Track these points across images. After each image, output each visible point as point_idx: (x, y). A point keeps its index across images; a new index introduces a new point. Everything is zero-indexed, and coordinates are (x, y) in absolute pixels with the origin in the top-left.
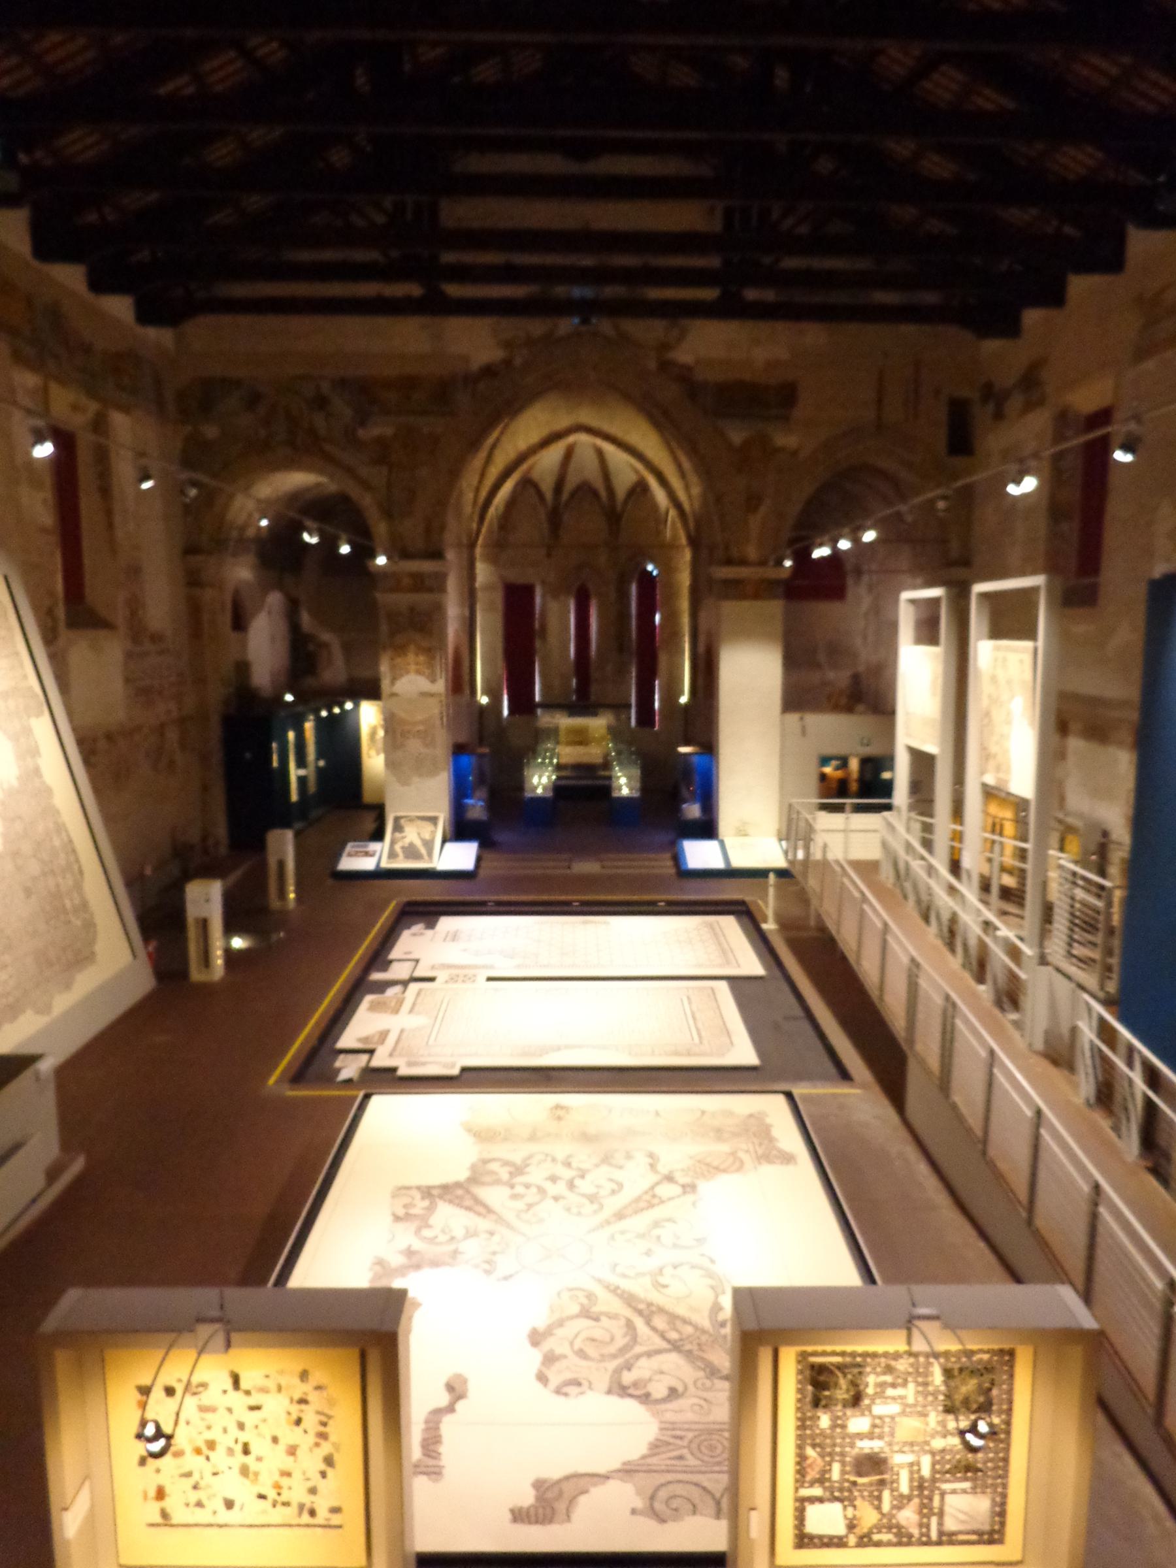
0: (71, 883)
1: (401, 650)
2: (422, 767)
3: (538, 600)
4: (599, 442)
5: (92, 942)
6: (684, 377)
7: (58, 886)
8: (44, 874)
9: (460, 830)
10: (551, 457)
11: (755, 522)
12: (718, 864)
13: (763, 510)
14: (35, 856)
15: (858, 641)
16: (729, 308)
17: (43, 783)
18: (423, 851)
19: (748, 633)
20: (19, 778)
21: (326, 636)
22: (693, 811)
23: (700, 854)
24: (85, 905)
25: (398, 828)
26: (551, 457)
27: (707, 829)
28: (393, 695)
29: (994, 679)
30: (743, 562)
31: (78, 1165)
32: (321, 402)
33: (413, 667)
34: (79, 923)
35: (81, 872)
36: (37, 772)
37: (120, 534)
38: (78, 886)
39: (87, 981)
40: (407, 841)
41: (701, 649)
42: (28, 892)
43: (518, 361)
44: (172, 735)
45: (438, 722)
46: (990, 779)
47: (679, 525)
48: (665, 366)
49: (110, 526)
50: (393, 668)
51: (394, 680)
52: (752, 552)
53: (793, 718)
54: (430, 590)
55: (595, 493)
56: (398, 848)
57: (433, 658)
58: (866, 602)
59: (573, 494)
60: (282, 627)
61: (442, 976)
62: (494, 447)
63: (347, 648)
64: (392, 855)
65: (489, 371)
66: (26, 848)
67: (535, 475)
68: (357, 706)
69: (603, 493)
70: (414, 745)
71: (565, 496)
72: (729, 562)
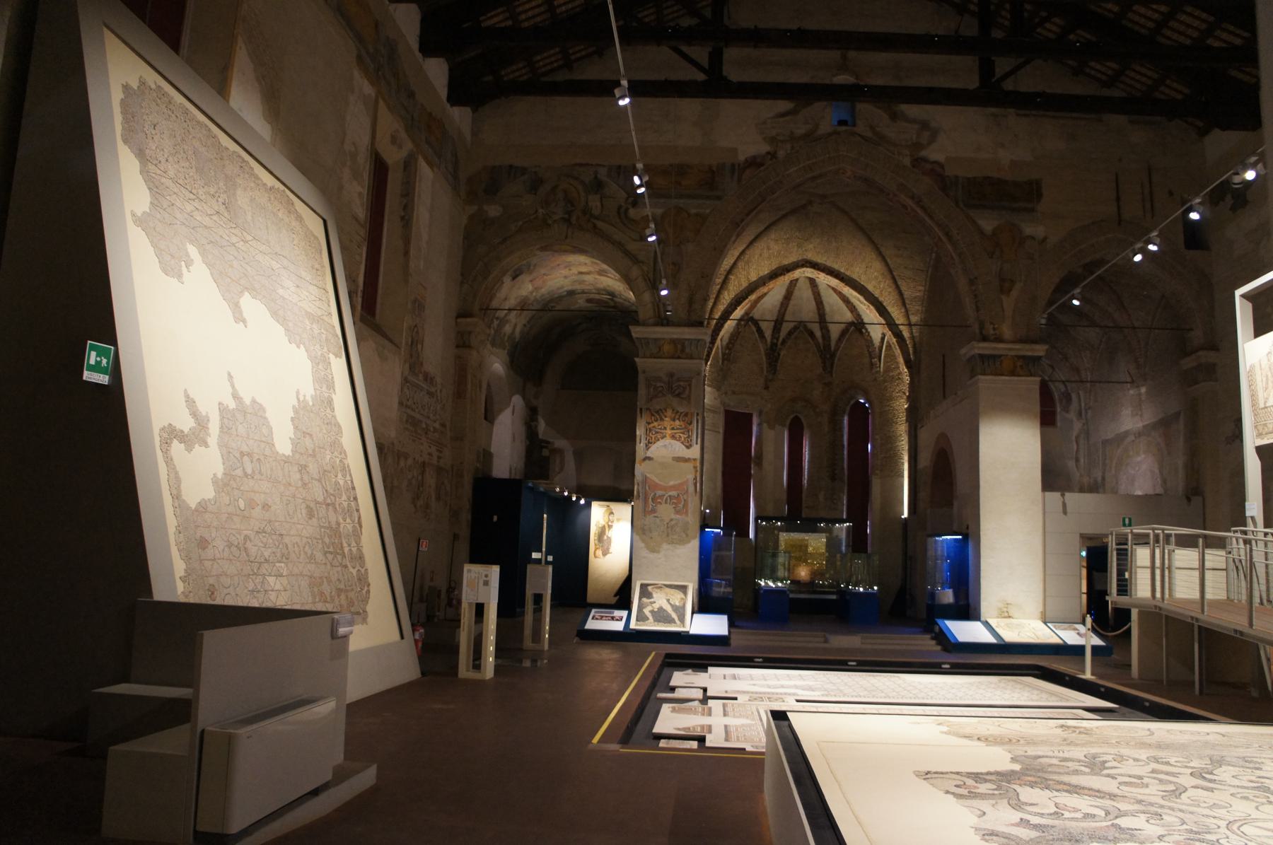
0: (350, 527)
1: (658, 414)
2: (672, 534)
3: (755, 428)
4: (823, 279)
5: (366, 600)
6: (937, 172)
9: (705, 605)
10: (776, 291)
11: (1008, 302)
12: (988, 638)
13: (1014, 293)
14: (319, 481)
15: (1071, 464)
16: (989, 94)
17: (334, 417)
18: (674, 616)
19: (1006, 408)
21: (560, 443)
22: (948, 596)
23: (965, 631)
24: (361, 558)
25: (645, 592)
26: (776, 291)
27: (967, 610)
28: (649, 459)
30: (999, 339)
31: (367, 778)
32: (598, 186)
33: (669, 432)
34: (354, 572)
36: (330, 402)
37: (412, 264)
40: (656, 606)
41: (925, 460)
42: (311, 514)
43: (781, 154)
44: (431, 480)
45: (691, 489)
47: (898, 351)
48: (917, 162)
49: (406, 253)
50: (648, 431)
51: (647, 447)
52: (1007, 332)
53: (1055, 496)
54: (692, 358)
55: (812, 334)
56: (647, 611)
57: (691, 423)
58: (1077, 426)
59: (790, 333)
60: (521, 430)
61: (742, 699)
62: (729, 272)
63: (579, 456)
64: (641, 618)
65: (754, 163)
66: (313, 468)
67: (756, 314)
68: (588, 505)
69: (818, 334)
70: (666, 511)
71: (783, 334)
72: (985, 339)
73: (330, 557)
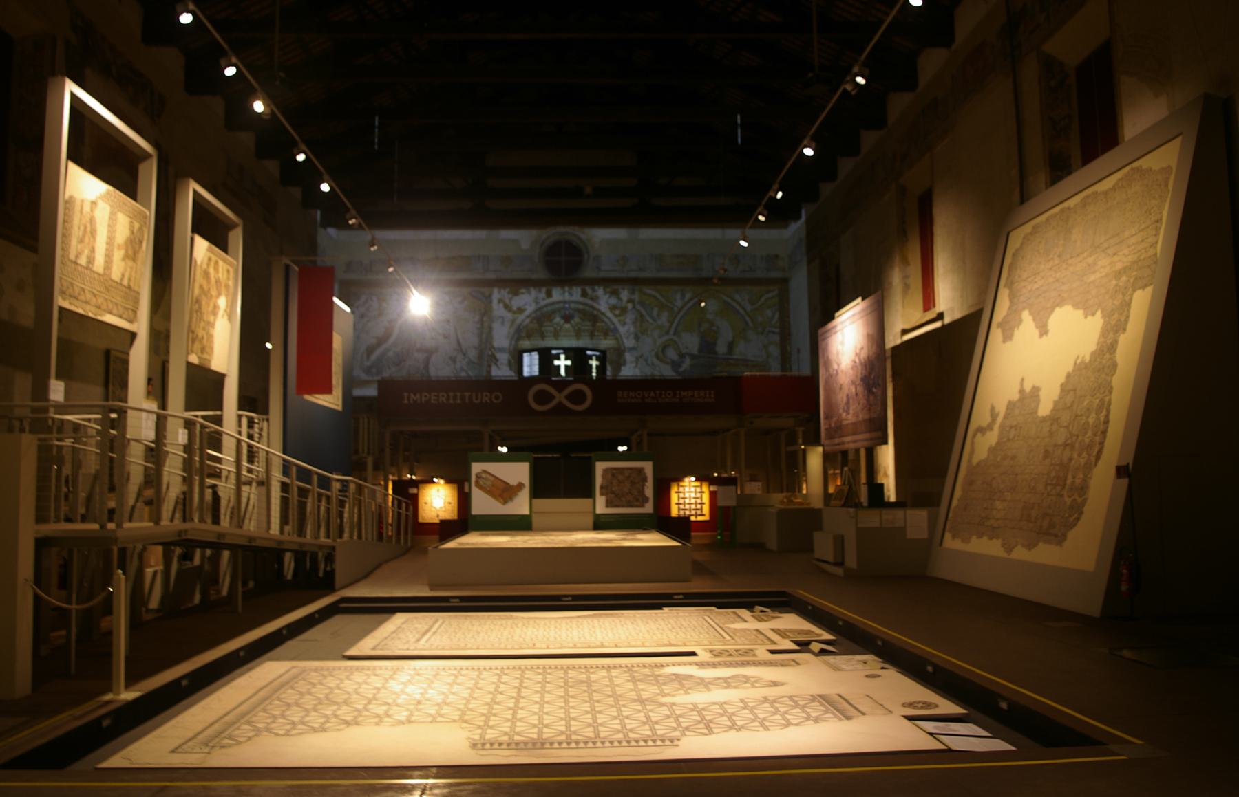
0: (1082, 461)
5: (1072, 526)
7: (1071, 459)
8: (1066, 445)
20: (1093, 354)
24: (1083, 489)
29: (206, 274)
34: (1068, 501)
35: (1098, 457)
36: (1112, 348)
38: (1088, 468)
39: (1045, 554)
42: (1047, 454)
46: (193, 359)
66: (1065, 418)
73: (1049, 488)
